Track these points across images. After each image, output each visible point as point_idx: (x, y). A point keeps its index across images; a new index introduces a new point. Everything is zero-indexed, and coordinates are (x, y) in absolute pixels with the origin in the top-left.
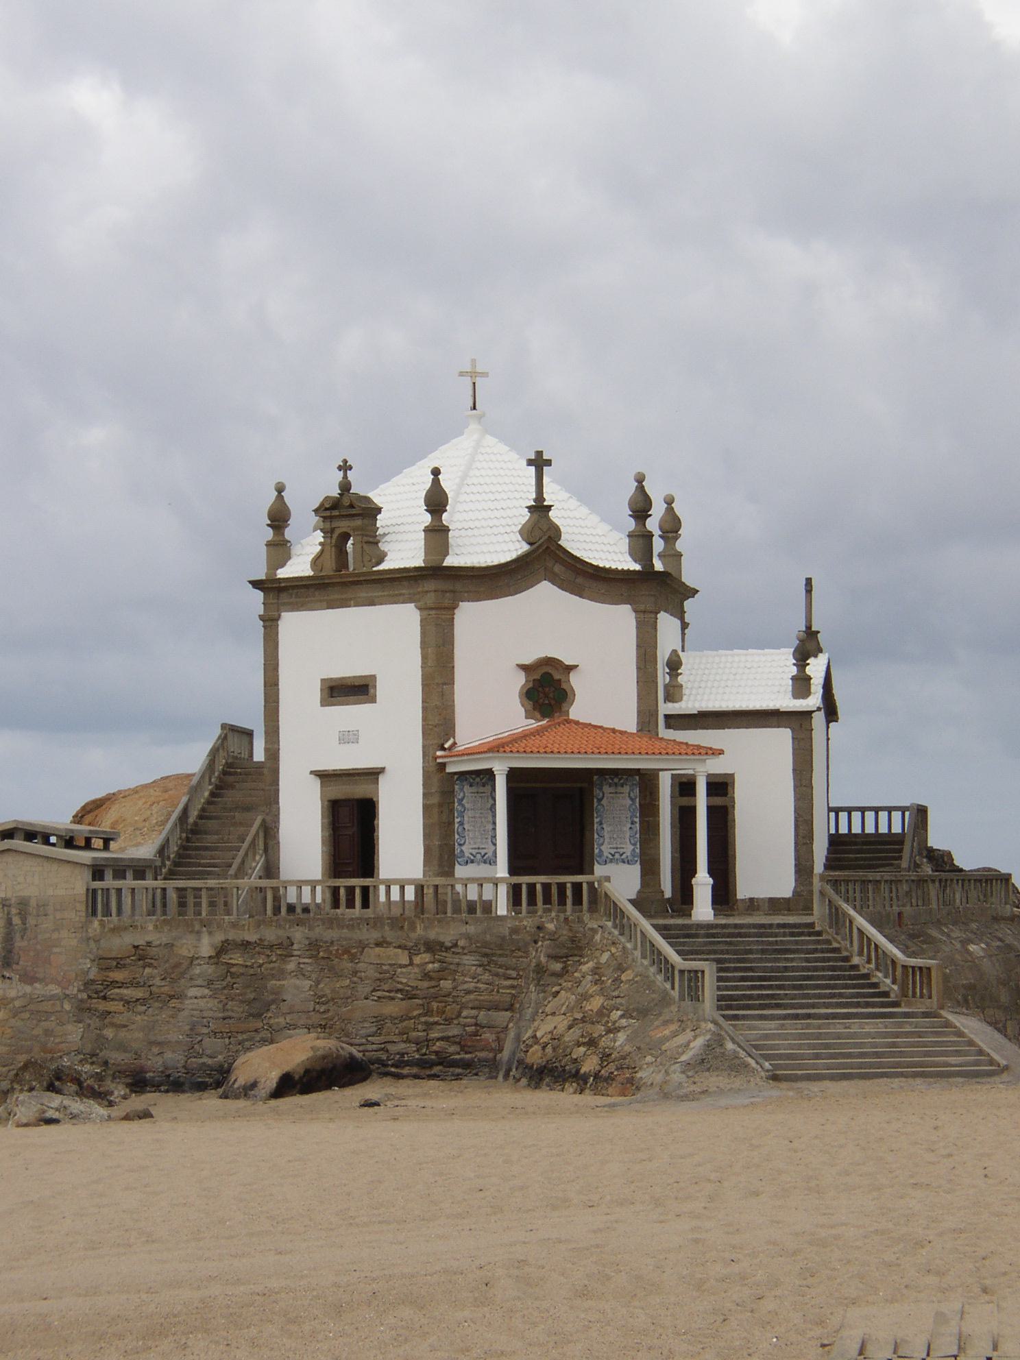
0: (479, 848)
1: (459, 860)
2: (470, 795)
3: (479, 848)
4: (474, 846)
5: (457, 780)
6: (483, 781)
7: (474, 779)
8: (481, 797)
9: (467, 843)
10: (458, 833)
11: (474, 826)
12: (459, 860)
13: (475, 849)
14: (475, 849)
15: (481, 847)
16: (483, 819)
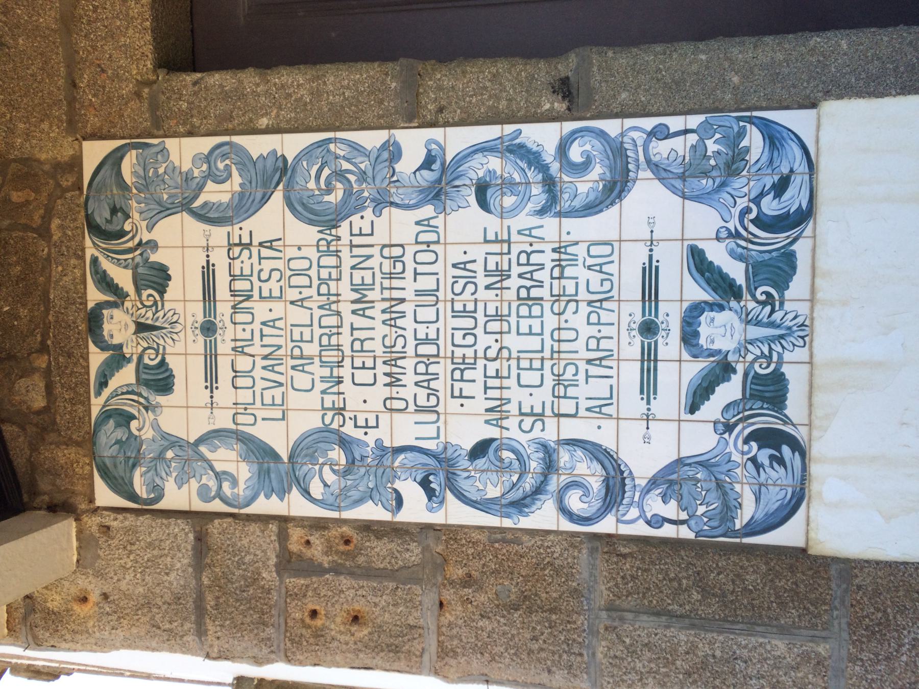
0: (649, 329)
1: (747, 511)
2: (225, 394)
3: (649, 329)
4: (631, 373)
5: (122, 487)
6: (123, 278)
7: (118, 359)
8: (241, 299)
9: (604, 437)
10: (521, 505)
11: (462, 366)
12: (747, 511)
13: (649, 358)
14: (649, 358)
15: (633, 312)
16: (408, 287)
